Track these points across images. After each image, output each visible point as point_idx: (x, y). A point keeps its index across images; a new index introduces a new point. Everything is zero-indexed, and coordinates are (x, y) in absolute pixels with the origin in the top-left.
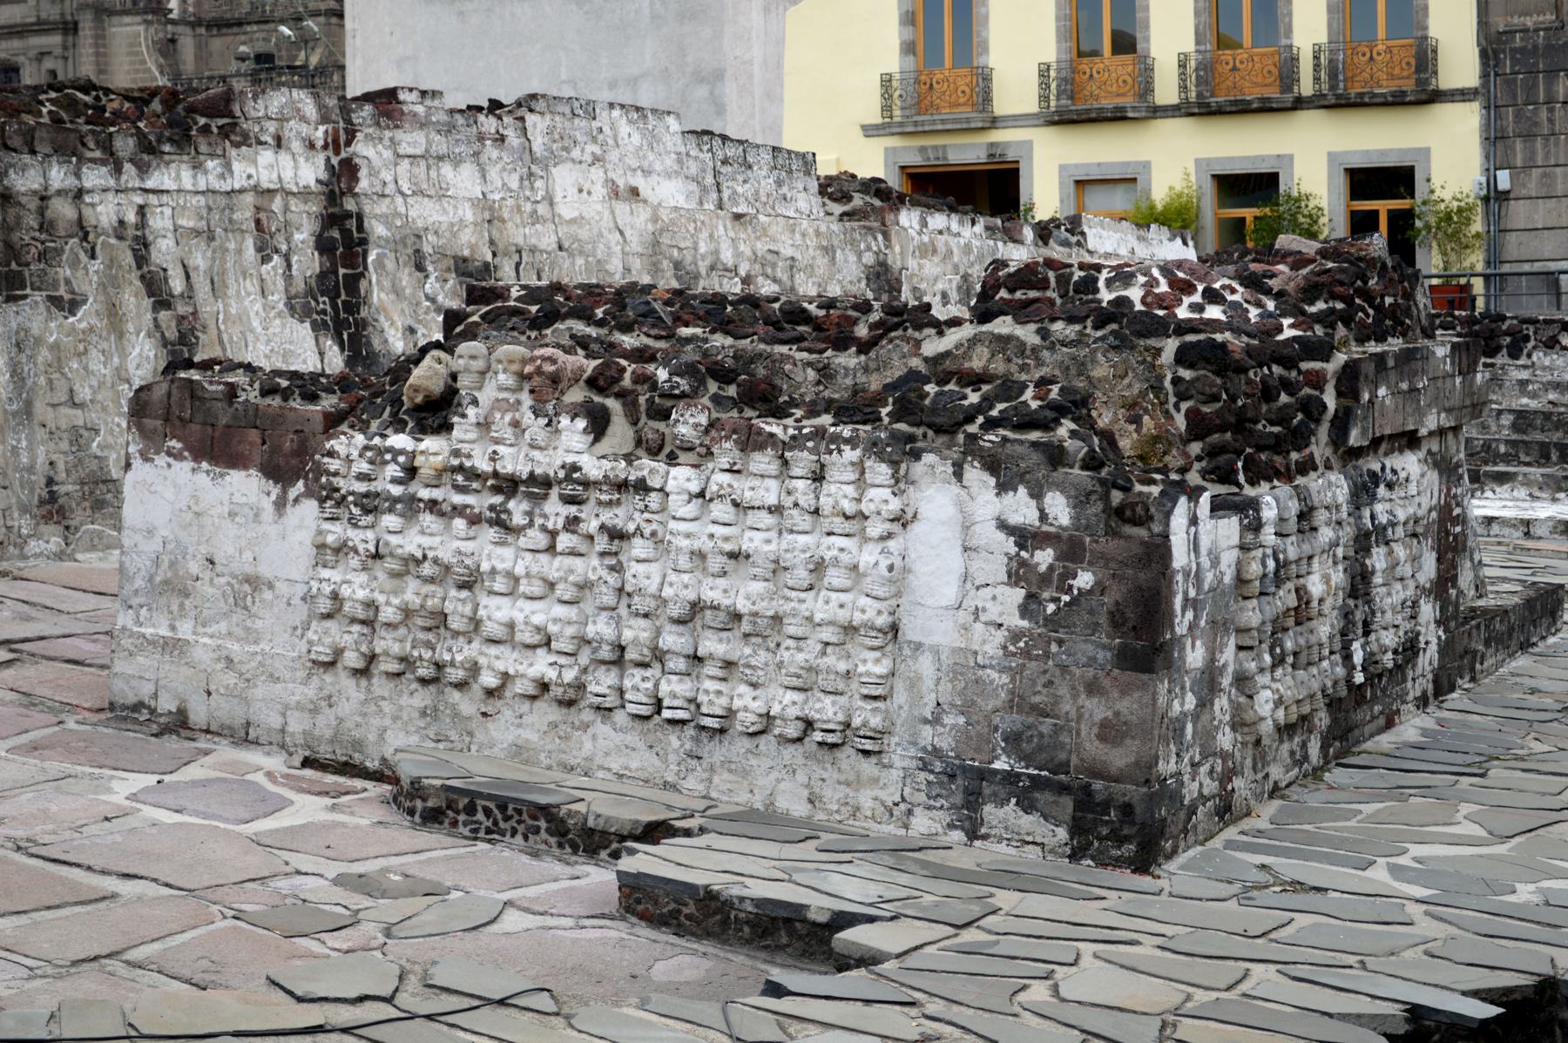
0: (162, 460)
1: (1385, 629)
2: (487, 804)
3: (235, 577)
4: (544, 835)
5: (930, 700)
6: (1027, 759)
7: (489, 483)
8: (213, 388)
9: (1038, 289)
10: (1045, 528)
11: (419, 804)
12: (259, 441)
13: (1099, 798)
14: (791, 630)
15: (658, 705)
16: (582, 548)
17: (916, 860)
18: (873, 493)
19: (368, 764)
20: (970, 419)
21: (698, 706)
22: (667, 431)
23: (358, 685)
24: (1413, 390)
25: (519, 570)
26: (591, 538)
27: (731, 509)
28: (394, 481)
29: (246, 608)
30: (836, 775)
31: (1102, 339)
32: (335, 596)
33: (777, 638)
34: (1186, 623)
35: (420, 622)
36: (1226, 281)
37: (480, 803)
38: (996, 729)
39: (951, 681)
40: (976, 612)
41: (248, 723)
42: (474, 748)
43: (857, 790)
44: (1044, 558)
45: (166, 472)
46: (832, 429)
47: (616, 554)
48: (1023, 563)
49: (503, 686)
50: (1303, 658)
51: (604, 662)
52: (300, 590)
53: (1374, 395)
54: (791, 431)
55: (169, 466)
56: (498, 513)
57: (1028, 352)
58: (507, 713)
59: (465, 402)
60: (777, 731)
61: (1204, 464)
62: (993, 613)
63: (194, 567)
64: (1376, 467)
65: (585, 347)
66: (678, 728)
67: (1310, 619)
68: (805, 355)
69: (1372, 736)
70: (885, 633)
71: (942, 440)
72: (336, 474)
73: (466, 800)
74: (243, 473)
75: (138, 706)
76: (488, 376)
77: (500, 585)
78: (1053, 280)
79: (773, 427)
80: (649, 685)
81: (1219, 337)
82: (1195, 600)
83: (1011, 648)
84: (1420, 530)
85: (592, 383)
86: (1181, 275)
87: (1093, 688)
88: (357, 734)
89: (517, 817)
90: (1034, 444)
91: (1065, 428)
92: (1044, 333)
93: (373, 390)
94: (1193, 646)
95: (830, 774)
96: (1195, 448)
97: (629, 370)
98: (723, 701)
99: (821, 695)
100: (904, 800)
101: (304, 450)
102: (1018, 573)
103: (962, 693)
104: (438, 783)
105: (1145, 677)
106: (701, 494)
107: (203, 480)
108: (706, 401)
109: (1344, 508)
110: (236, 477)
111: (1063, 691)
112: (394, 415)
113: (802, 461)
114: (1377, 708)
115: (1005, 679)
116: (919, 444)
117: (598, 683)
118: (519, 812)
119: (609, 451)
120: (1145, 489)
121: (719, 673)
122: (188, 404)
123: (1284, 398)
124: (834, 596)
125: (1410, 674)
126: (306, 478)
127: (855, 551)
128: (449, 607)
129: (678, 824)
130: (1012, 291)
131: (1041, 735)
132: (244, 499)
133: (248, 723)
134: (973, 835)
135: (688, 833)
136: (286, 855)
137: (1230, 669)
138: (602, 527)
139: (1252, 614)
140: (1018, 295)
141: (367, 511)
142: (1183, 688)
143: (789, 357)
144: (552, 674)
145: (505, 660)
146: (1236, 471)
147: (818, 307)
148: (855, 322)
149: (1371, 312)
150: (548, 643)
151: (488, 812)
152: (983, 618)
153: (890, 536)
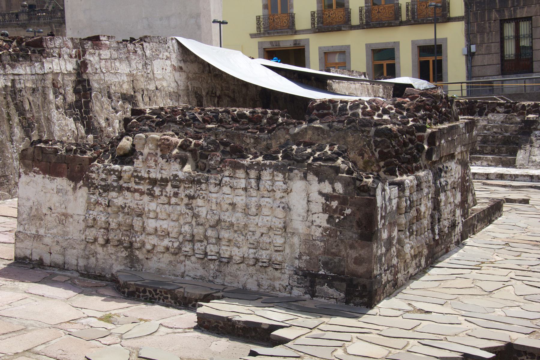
0: (32, 174)
1: (445, 220)
2: (150, 289)
3: (59, 214)
4: (169, 299)
5: (298, 251)
6: (331, 270)
7: (147, 181)
8: (50, 150)
9: (327, 110)
10: (335, 194)
11: (126, 290)
12: (66, 167)
13: (355, 283)
14: (251, 229)
15: (206, 254)
16: (179, 203)
17: (295, 305)
18: (277, 183)
19: (107, 276)
20: (308, 158)
21: (220, 254)
22: (207, 163)
23: (103, 250)
24: (453, 140)
27: (230, 189)
29: (63, 224)
31: (350, 128)
32: (94, 219)
33: (246, 232)
34: (382, 223)
35: (124, 228)
36: (390, 106)
37: (148, 289)
38: (320, 260)
39: (304, 245)
40: (312, 222)
41: (65, 263)
42: (143, 270)
43: (274, 282)
44: (335, 204)
45: (34, 179)
46: (263, 162)
47: (191, 204)
48: (328, 206)
49: (153, 249)
50: (419, 232)
51: (187, 241)
52: (82, 218)
53: (440, 143)
54: (249, 163)
55: (35, 176)
56: (150, 191)
57: (325, 132)
58: (155, 258)
60: (246, 263)
61: (385, 169)
62: (318, 222)
63: (45, 211)
64: (441, 167)
66: (213, 262)
67: (421, 219)
68: (250, 134)
69: (441, 256)
70: (282, 230)
72: (94, 179)
73: (143, 288)
74: (61, 178)
75: (25, 258)
76: (146, 145)
77: (152, 215)
78: (332, 107)
80: (203, 248)
81: (389, 126)
82: (384, 216)
83: (324, 234)
84: (456, 186)
86: (375, 104)
87: (352, 247)
88: (103, 266)
89: (160, 294)
90: (330, 166)
91: (340, 160)
92: (330, 126)
93: (105, 149)
94: (384, 231)
95: (265, 276)
96: (382, 164)
97: (193, 142)
98: (229, 253)
99: (261, 250)
101: (82, 171)
102: (326, 209)
103: (308, 249)
105: (369, 243)
107: (47, 181)
109: (431, 181)
110: (59, 180)
111: (342, 247)
113: (253, 174)
114: (443, 246)
117: (186, 247)
118: (161, 292)
120: (367, 180)
121: (227, 244)
122: (41, 154)
123: (410, 145)
124: (265, 217)
125: (453, 234)
126: (83, 180)
127: (271, 202)
129: (214, 295)
130: (318, 111)
131: (335, 262)
132: (61, 188)
133: (65, 263)
134: (313, 295)
135: (218, 298)
136: (83, 310)
137: (396, 238)
138: (186, 195)
139: (403, 220)
140: (320, 112)
141: (105, 191)
142: (381, 246)
144: (170, 244)
145: (152, 240)
146: (395, 171)
148: (263, 117)
149: (438, 114)
150: (168, 234)
151: (150, 292)
152: (315, 224)
153: (283, 197)
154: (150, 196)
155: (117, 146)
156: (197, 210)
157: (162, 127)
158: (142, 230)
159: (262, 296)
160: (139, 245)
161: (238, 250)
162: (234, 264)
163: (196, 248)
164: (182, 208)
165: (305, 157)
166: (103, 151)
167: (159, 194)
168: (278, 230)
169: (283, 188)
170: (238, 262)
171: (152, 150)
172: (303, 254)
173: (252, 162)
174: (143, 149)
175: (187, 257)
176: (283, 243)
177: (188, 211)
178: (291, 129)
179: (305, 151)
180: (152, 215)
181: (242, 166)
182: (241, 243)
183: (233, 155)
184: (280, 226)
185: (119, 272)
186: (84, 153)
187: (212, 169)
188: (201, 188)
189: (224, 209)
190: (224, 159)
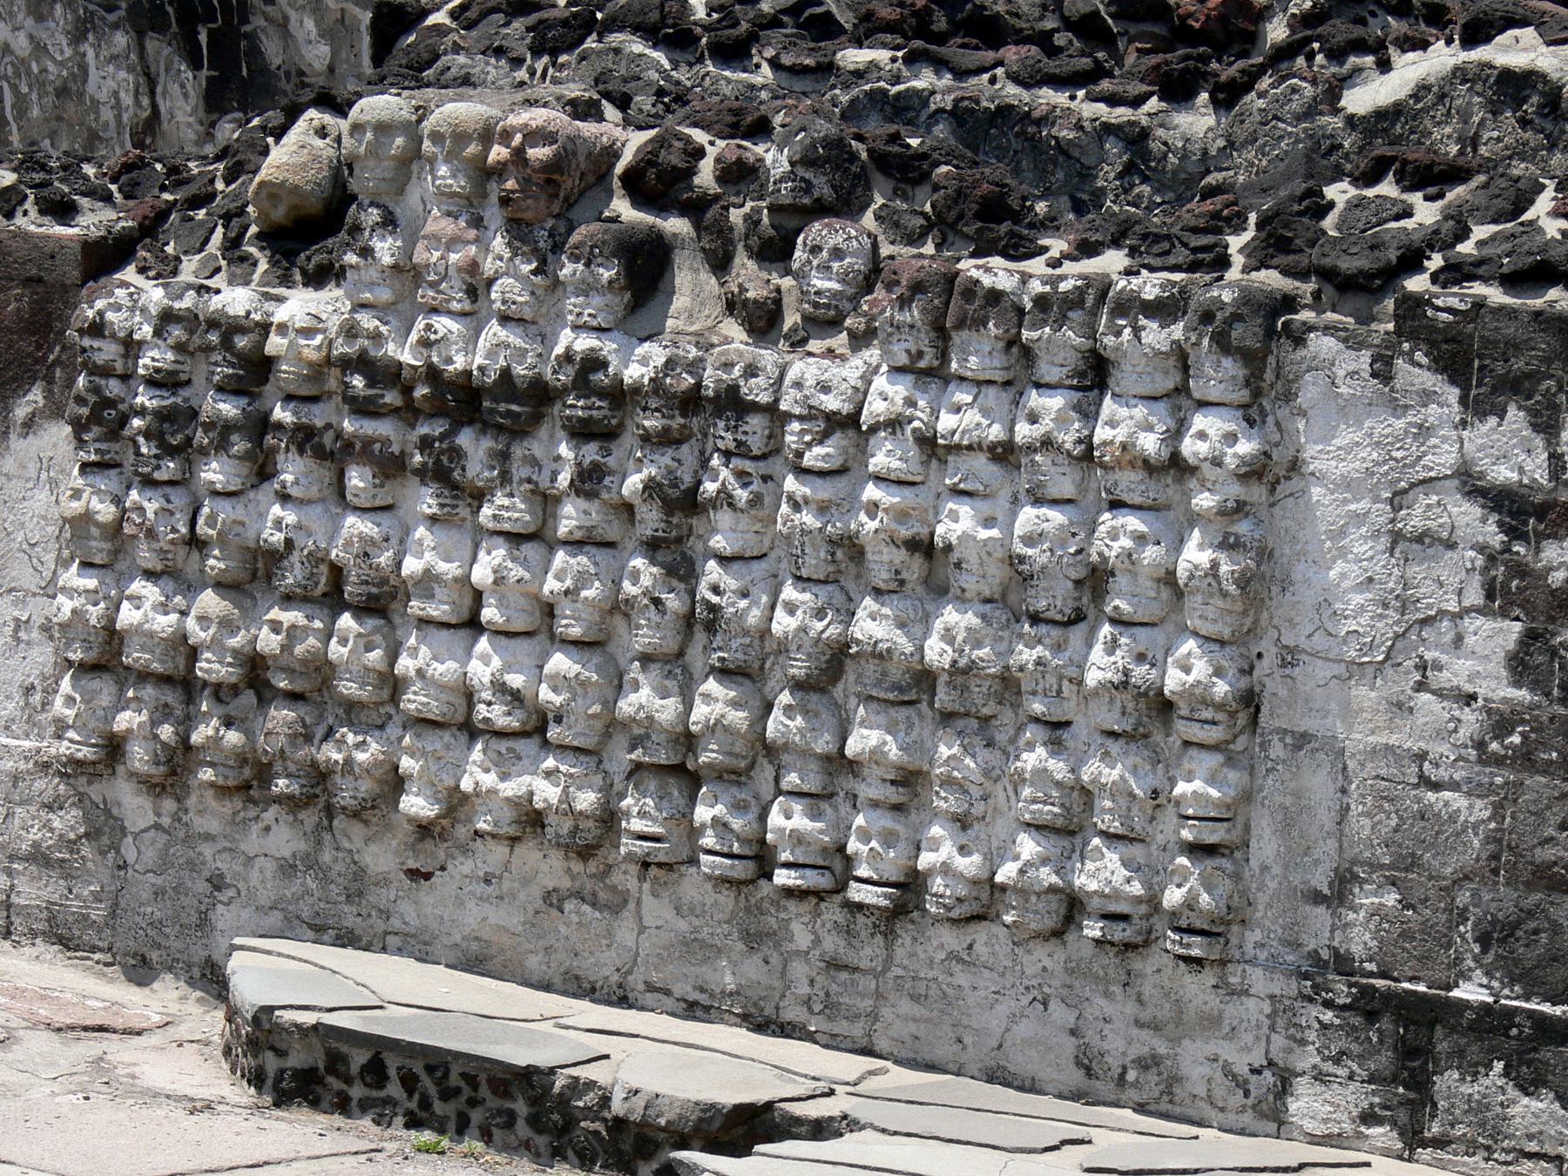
11: (271, 1063)
15: (762, 859)
16: (613, 532)
20: (1412, 261)
25: (481, 574)
26: (627, 509)
28: (226, 389)
30: (1131, 1008)
39: (1368, 815)
47: (679, 540)
48: (1519, 570)
54: (1037, 287)
62: (1458, 671)
65: (623, 103)
66: (807, 905)
68: (1101, 108)
70: (1232, 715)
72: (106, 371)
76: (415, 167)
79: (997, 274)
89: (467, 1092)
95: (1121, 1008)
97: (712, 152)
100: (1271, 1064)
104: (308, 1018)
112: (233, 244)
115: (1481, 810)
116: (1306, 315)
121: (893, 795)
126: (50, 380)
128: (336, 651)
129: (798, 1109)
135: (820, 1130)
150: (541, 729)
151: (409, 1082)
155: (255, 172)
158: (386, 694)
159: (1093, 1133)
160: (366, 787)
162: (937, 920)
165: (1393, 255)
168: (1207, 714)
170: (954, 914)
174: (401, 192)
175: (653, 871)
179: (1397, 218)
188: (739, 444)
189: (881, 576)
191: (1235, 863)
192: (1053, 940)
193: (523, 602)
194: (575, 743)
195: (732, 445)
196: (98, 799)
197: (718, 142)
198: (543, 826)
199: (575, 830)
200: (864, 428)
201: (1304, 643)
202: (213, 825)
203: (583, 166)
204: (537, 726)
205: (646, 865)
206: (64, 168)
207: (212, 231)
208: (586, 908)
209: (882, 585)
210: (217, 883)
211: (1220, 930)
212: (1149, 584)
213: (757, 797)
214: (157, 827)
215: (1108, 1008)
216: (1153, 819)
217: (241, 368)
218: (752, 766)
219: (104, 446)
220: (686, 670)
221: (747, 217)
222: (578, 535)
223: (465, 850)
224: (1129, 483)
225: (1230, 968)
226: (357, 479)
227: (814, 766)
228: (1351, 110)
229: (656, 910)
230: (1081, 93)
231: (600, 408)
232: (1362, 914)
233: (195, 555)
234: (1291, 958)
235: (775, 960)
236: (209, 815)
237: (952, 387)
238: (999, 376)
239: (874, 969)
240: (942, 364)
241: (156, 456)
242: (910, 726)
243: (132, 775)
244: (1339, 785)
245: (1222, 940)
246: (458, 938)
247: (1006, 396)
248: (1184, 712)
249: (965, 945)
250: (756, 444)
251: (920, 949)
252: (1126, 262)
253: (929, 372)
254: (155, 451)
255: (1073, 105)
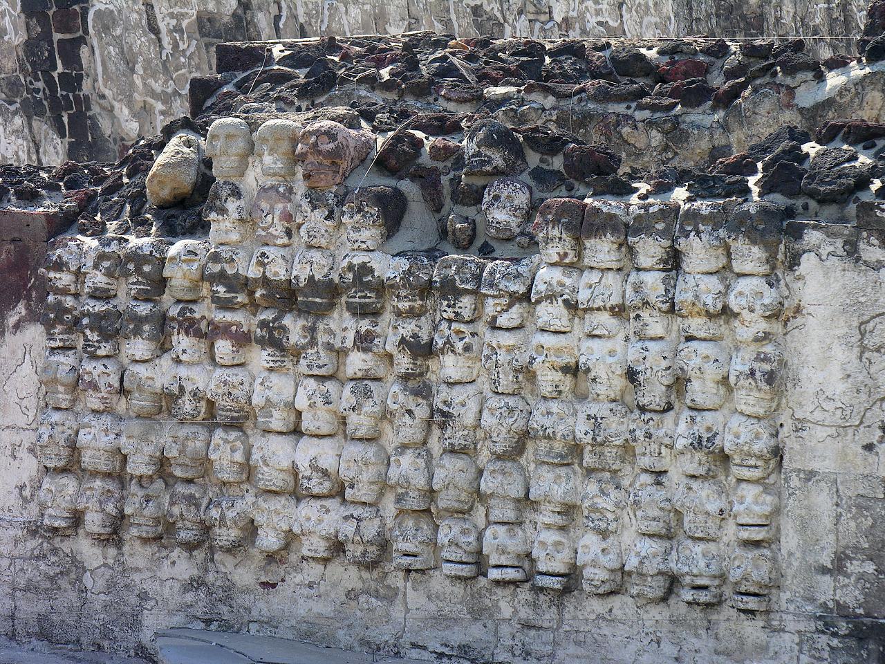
15: (480, 563)
16: (381, 372)
18: (743, 285)
22: (478, 219)
30: (712, 643)
47: (421, 374)
59: (224, 194)
60: (634, 591)
65: (369, 117)
66: (509, 590)
68: (646, 114)
70: (767, 461)
71: (831, 210)
72: (65, 292)
76: (250, 160)
79: (610, 205)
85: (383, 164)
99: (690, 543)
103: (869, 533)
106: (526, 297)
108: (525, 177)
112: (135, 214)
113: (650, 250)
117: (405, 540)
119: (408, 247)
121: (559, 520)
126: (29, 298)
138: (403, 341)
143: (627, 117)
144: (349, 529)
147: (661, 53)
154: (270, 350)
156: (443, 396)
157: (322, 100)
158: (244, 477)
160: (234, 534)
161: (604, 545)
163: (446, 541)
164: (394, 393)
165: (852, 181)
166: (99, 189)
167: (304, 341)
168: (752, 462)
169: (767, 301)
170: (601, 591)
171: (275, 175)
172: (848, 552)
173: (646, 207)
174: (242, 174)
175: (413, 575)
176: (771, 514)
177: (411, 402)
178: (803, 87)
180: (278, 420)
181: (607, 224)
182: (610, 516)
183: (576, 185)
184: (757, 447)
185: (163, 635)
186: (31, 197)
187: (497, 239)
188: (457, 314)
189: (546, 389)
190: (542, 200)
191: (772, 551)
192: (662, 604)
193: (327, 417)
194: (363, 500)
195: (452, 316)
196: (67, 551)
197: (431, 138)
198: (344, 552)
199: (364, 554)
200: (533, 301)
201: (808, 416)
202: (140, 562)
203: (352, 154)
204: (339, 492)
205: (408, 571)
206: (29, 173)
207: (122, 207)
208: (373, 600)
209: (548, 395)
210: (143, 596)
211: (766, 592)
212: (712, 385)
213: (475, 527)
214: (105, 565)
215: (698, 644)
216: (721, 527)
217: (149, 285)
218: (471, 508)
219: (65, 337)
220: (428, 452)
221: (451, 180)
222: (360, 374)
223: (297, 569)
224: (697, 325)
225: (772, 616)
226: (223, 347)
227: (511, 506)
228: (801, 105)
229: (415, 598)
230: (634, 105)
231: (370, 297)
232: (853, 579)
233: (124, 400)
234: (809, 608)
235: (490, 624)
236: (137, 555)
237: (586, 273)
238: (614, 265)
239: (552, 627)
240: (579, 260)
241: (97, 341)
242: (569, 479)
243: (88, 534)
244: (835, 501)
245: (767, 599)
246: (294, 622)
247: (619, 277)
248: (737, 461)
249: (607, 610)
250: (467, 314)
251: (579, 613)
252: (687, 194)
253: (571, 266)
254: (96, 338)
255: (629, 112)
